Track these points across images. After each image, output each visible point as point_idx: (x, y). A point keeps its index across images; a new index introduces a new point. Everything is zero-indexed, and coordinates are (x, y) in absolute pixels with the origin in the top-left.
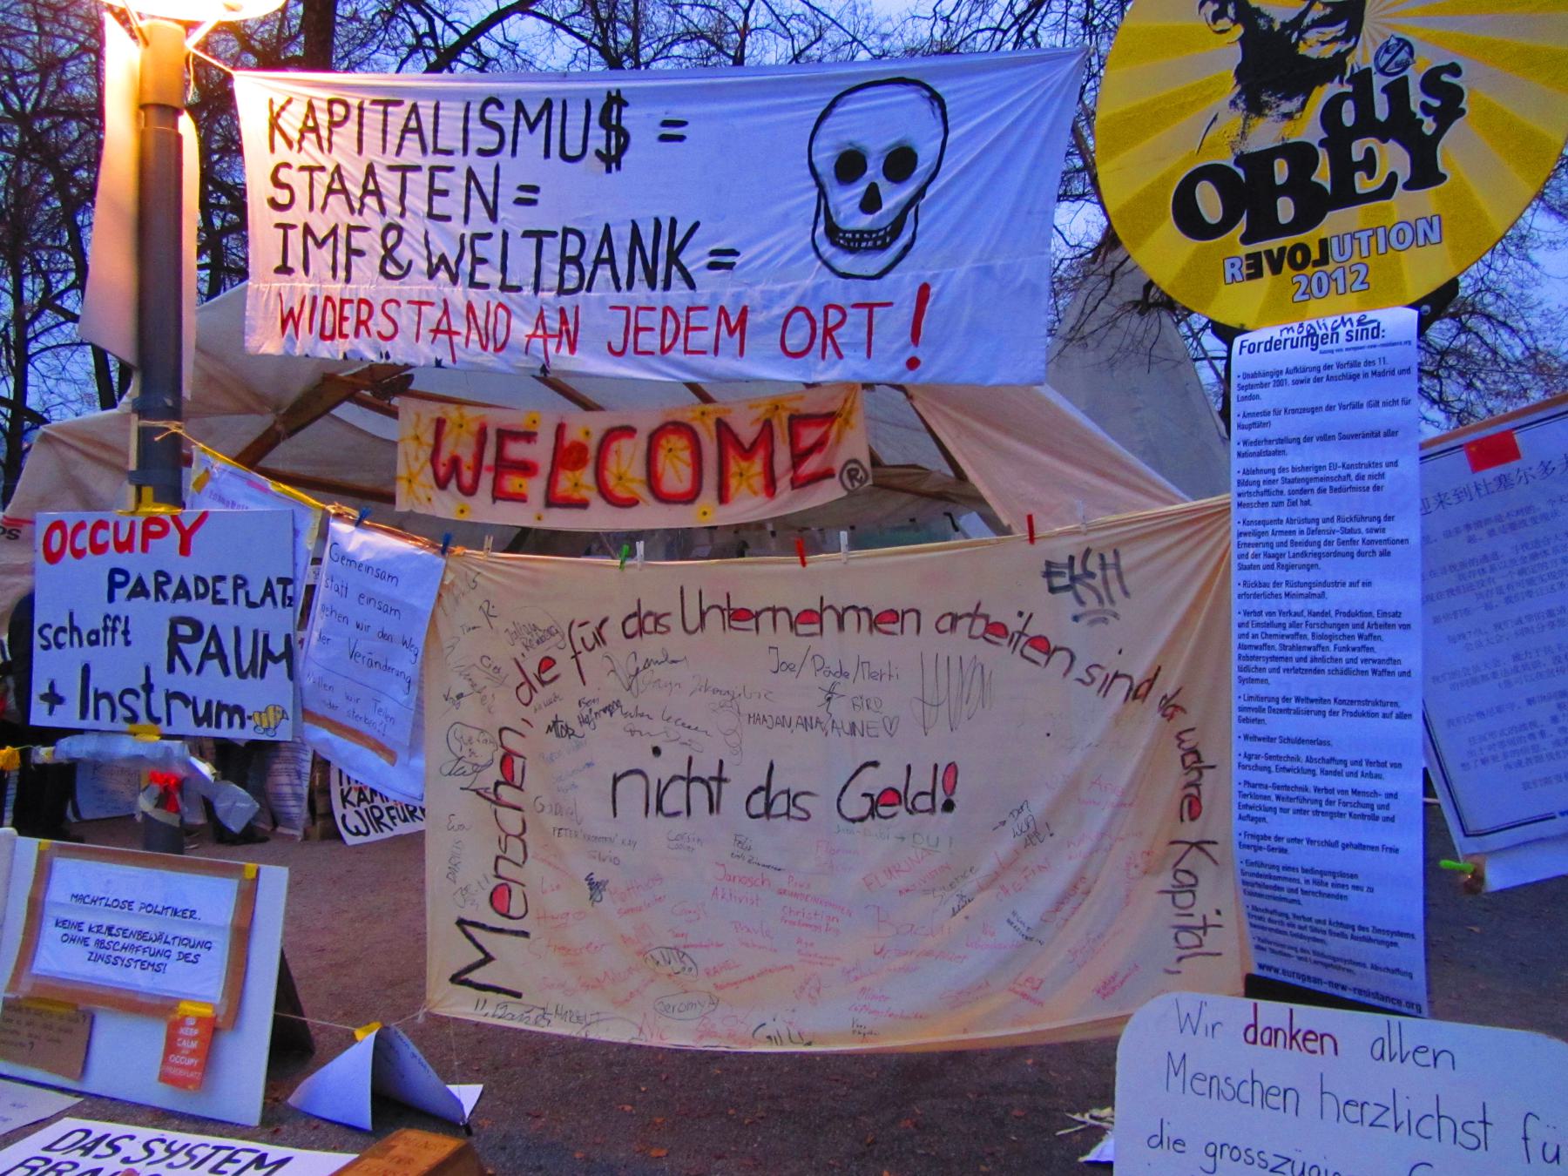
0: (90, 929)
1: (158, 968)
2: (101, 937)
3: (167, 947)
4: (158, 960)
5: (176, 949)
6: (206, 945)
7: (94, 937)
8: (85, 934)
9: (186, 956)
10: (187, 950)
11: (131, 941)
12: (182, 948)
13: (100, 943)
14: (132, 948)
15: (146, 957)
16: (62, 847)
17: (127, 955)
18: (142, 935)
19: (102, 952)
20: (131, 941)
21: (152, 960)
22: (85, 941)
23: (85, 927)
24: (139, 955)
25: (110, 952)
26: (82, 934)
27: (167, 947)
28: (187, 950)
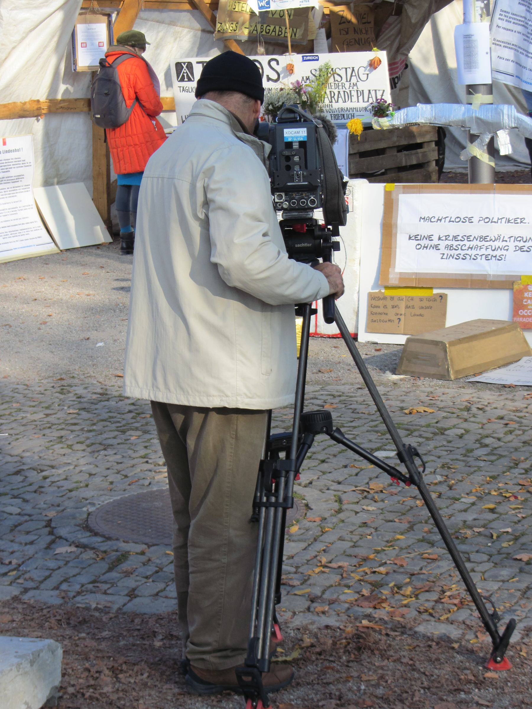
0: (439, 239)
2: (449, 243)
3: (504, 244)
4: (498, 253)
5: (512, 245)
7: (443, 244)
8: (436, 242)
9: (521, 248)
10: (521, 244)
12: (517, 243)
13: (450, 247)
14: (477, 247)
15: (489, 251)
16: (404, 187)
17: (473, 252)
18: (484, 238)
19: (453, 252)
22: (436, 247)
23: (435, 238)
24: (483, 251)
25: (459, 251)
26: (432, 243)
28: (521, 244)
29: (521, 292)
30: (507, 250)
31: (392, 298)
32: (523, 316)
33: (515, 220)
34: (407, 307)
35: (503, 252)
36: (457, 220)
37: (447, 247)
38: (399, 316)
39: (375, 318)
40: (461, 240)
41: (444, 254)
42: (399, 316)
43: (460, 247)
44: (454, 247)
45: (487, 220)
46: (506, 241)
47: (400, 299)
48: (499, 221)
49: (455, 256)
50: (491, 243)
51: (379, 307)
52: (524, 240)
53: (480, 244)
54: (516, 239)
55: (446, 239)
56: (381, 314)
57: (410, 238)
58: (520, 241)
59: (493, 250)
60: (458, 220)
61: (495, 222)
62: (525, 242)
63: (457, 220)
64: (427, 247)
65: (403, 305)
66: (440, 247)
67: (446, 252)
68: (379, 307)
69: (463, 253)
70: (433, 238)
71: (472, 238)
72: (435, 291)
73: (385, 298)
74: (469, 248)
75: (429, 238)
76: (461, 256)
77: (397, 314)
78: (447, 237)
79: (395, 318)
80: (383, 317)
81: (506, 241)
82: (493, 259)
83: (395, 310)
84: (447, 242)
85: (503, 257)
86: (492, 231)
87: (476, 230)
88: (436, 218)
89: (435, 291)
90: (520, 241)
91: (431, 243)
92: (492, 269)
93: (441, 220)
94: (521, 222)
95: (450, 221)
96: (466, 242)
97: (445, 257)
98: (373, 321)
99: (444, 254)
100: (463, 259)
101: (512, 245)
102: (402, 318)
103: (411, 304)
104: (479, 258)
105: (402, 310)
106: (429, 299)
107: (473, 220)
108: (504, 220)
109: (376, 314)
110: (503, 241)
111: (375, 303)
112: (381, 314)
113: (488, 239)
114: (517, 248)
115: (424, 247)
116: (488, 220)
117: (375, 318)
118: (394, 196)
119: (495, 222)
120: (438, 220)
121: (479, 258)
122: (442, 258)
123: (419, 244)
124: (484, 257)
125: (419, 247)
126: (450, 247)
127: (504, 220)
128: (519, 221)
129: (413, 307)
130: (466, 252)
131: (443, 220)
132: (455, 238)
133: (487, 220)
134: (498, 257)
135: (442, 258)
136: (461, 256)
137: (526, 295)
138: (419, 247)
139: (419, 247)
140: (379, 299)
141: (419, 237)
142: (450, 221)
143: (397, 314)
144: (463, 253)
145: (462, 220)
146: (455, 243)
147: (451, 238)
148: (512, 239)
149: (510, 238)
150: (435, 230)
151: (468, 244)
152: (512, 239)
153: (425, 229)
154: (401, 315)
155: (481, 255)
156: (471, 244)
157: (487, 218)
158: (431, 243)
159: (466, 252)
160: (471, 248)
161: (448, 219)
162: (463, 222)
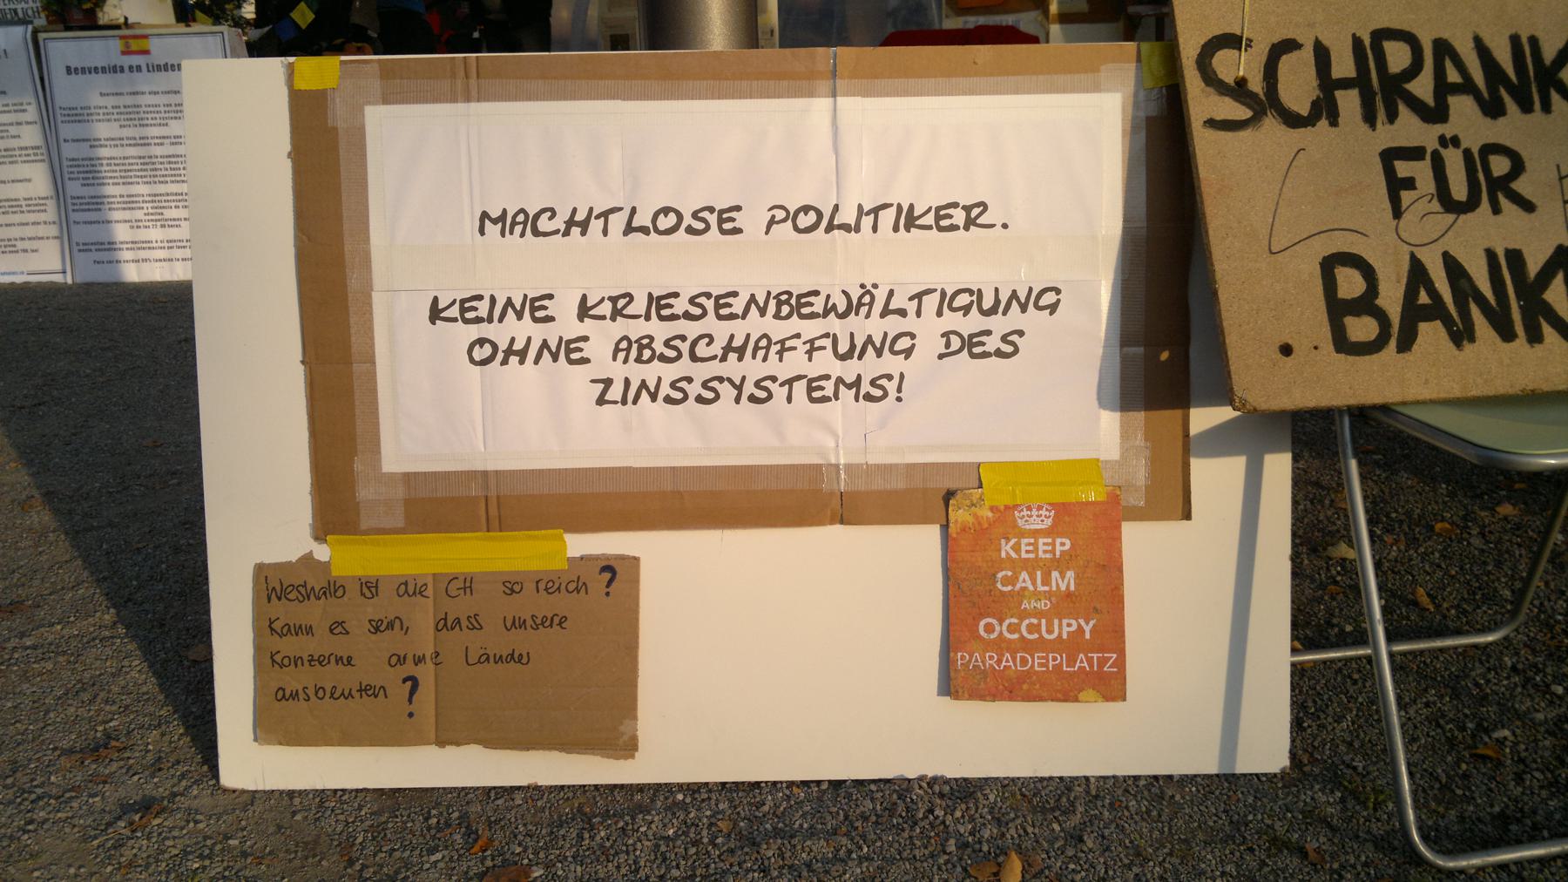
0: (584, 311)
1: (872, 392)
2: (637, 329)
3: (894, 324)
4: (870, 366)
6: (1044, 300)
7: (601, 338)
8: (568, 325)
10: (971, 324)
11: (755, 325)
12: (952, 320)
13: (640, 349)
14: (763, 345)
15: (825, 362)
17: (752, 368)
18: (794, 304)
20: (755, 325)
21: (850, 370)
22: (571, 351)
23: (564, 309)
24: (796, 362)
25: (684, 367)
26: (551, 333)
27: (894, 324)
29: (984, 535)
30: (908, 353)
31: (370, 587)
32: (1000, 645)
33: (940, 213)
34: (444, 624)
35: (891, 364)
36: (666, 222)
37: (623, 347)
38: (410, 669)
39: (294, 680)
40: (687, 316)
41: (608, 383)
42: (410, 669)
43: (685, 347)
44: (659, 347)
45: (805, 220)
46: (902, 313)
47: (409, 588)
48: (867, 222)
49: (666, 389)
50: (833, 324)
51: (310, 630)
52: (988, 303)
53: (779, 330)
54: (947, 302)
55: (617, 313)
56: (321, 661)
57: (435, 314)
58: (966, 309)
59: (843, 358)
60: (669, 222)
61: (845, 227)
62: (993, 311)
63: (666, 222)
64: (522, 355)
65: (422, 617)
66: (588, 350)
67: (617, 371)
68: (310, 630)
69: (702, 372)
70: (552, 308)
71: (738, 305)
72: (581, 545)
73: (333, 589)
74: (728, 349)
75: (536, 307)
76: (694, 389)
77: (402, 660)
78: (619, 306)
79: (392, 678)
80: (331, 676)
81: (902, 313)
82: (847, 395)
83: (389, 642)
84: (620, 327)
85: (891, 386)
86: (833, 267)
87: (754, 265)
88: (563, 216)
89: (581, 545)
90: (966, 309)
91: (538, 333)
92: (837, 436)
93: (584, 226)
94: (970, 223)
95: (629, 229)
96: (710, 324)
97: (615, 392)
98: (283, 695)
99: (608, 383)
100: (700, 399)
101: (929, 328)
102: (426, 673)
103: (461, 607)
104: (780, 393)
105: (424, 637)
106: (548, 584)
107: (741, 219)
108: (887, 217)
109: (297, 661)
110: (885, 312)
111: (284, 612)
112: (321, 661)
113: (818, 304)
114: (956, 343)
115: (509, 352)
116: (812, 217)
117: (294, 680)
118: (339, 114)
119: (845, 227)
120: (571, 223)
121: (780, 393)
122: (601, 401)
123: (481, 342)
124: (800, 388)
125: (481, 353)
126: (635, 349)
127: (887, 217)
128: (959, 217)
129: (475, 624)
130: (715, 368)
131: (596, 225)
132: (659, 305)
133: (805, 220)
134: (865, 387)
135: (601, 401)
136: (694, 389)
137: (1006, 549)
138: (481, 353)
139: (486, 354)
140: (306, 594)
141: (483, 308)
142: (629, 229)
143: (402, 660)
144: (702, 372)
145: (688, 220)
146: (660, 331)
147: (639, 306)
148: (931, 302)
149: (919, 296)
150: (570, 270)
151: (721, 331)
152: (931, 302)
153: (511, 268)
154: (419, 660)
155: (790, 382)
156: (739, 329)
157: (806, 209)
158: (538, 333)
159: (715, 368)
160: (741, 352)
161: (617, 222)
162: (690, 230)
